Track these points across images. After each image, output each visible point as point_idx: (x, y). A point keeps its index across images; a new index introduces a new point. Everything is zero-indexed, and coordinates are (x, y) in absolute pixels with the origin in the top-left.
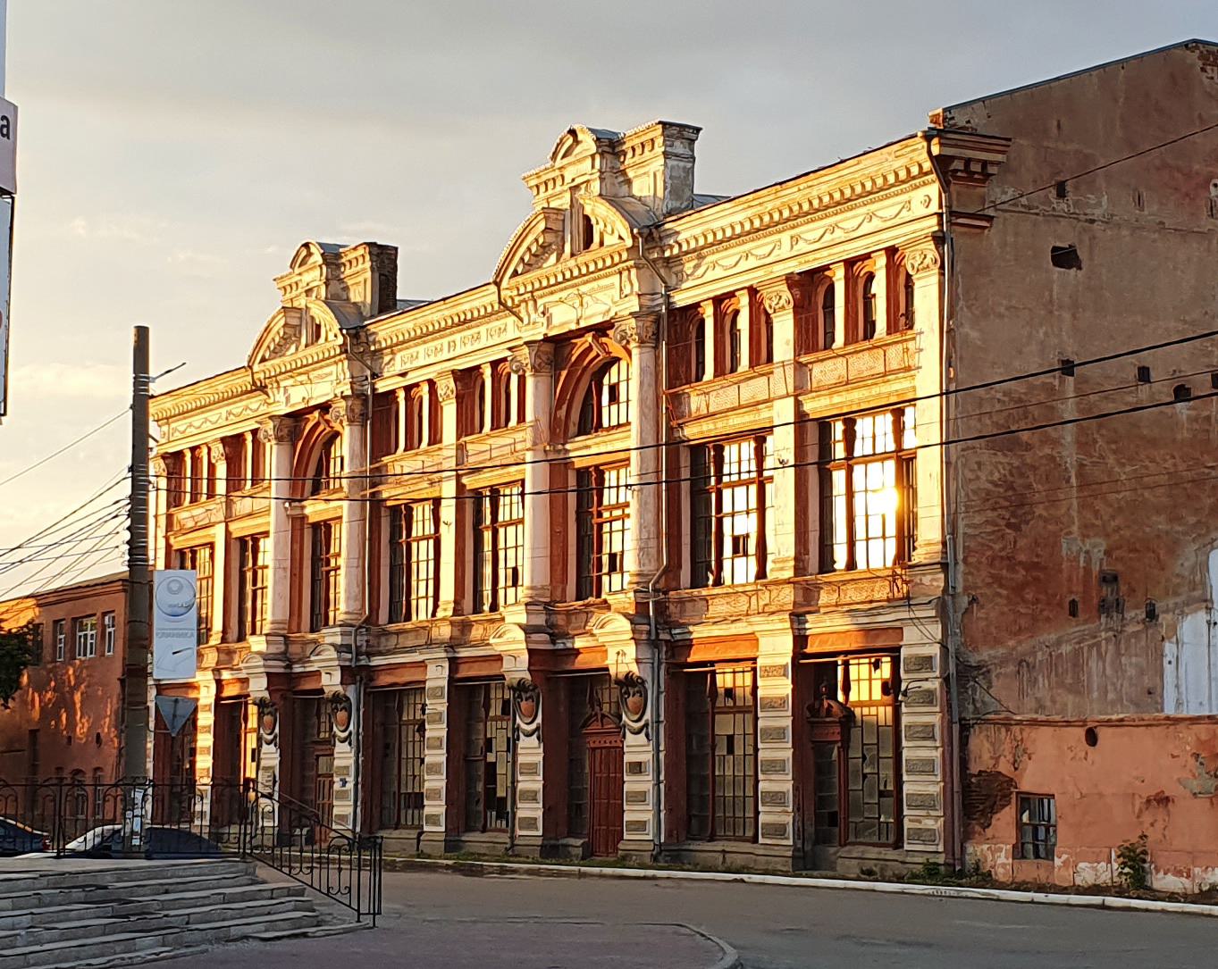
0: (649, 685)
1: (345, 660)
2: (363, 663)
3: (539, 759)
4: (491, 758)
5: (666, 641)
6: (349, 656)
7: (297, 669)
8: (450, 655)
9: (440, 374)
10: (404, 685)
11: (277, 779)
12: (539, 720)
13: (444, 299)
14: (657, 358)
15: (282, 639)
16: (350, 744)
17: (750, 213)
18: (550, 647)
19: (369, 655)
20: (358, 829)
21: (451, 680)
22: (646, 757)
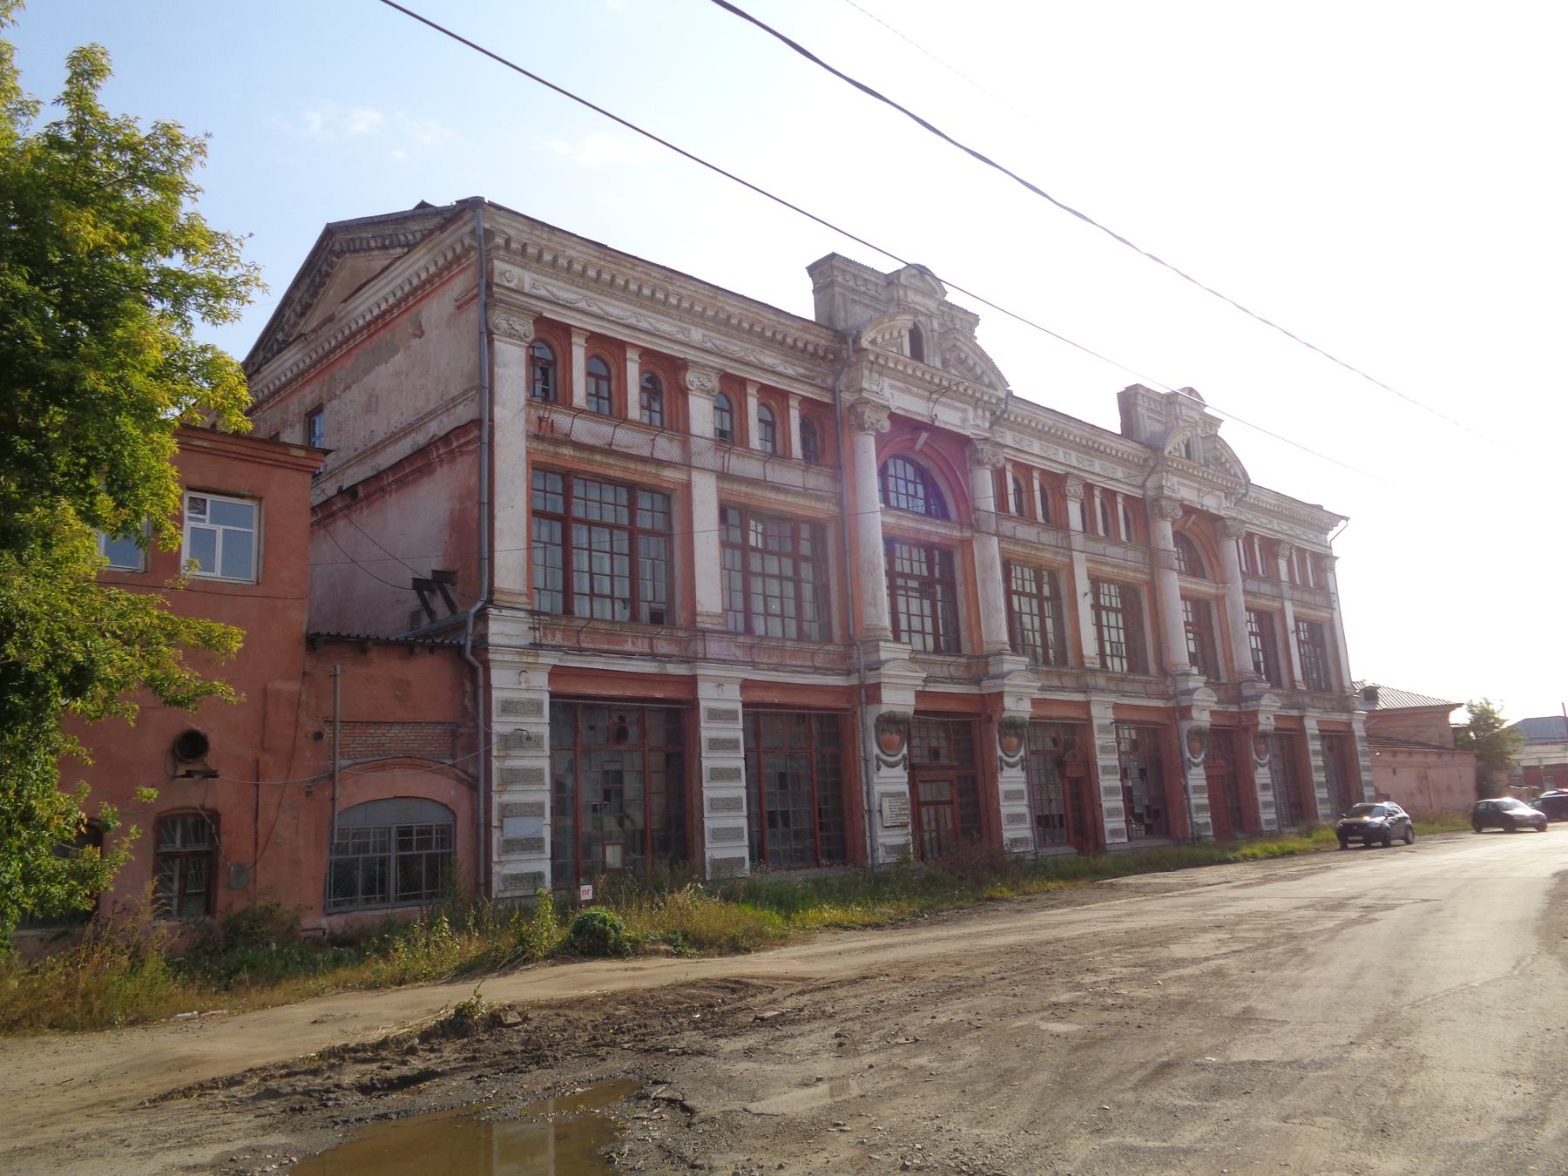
8: (1115, 700)
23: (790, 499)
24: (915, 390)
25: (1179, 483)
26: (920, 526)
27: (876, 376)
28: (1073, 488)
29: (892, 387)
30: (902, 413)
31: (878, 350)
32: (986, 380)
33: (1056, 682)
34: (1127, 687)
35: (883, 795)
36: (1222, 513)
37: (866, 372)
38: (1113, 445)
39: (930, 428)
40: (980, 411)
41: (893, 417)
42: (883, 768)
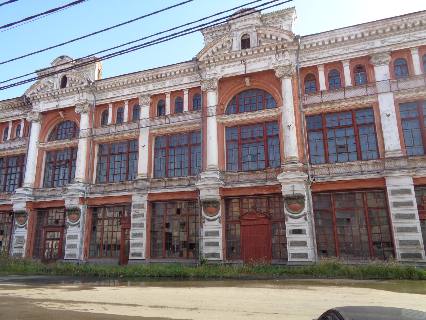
0: (306, 199)
1: (82, 195)
2: (89, 196)
3: (220, 231)
4: (170, 230)
5: (312, 183)
6: (83, 194)
7: (42, 200)
8: (149, 192)
9: (142, 96)
10: (111, 204)
11: (26, 241)
12: (220, 213)
13: (151, 70)
14: (293, 84)
15: (32, 189)
16: (79, 227)
17: (363, 31)
18: (223, 187)
19: (91, 194)
20: (82, 259)
21: (148, 202)
22: (307, 229)
23: (15, 150)
24: (52, 100)
25: (223, 68)
26: (60, 144)
27: (37, 103)
28: (141, 102)
29: (44, 103)
30: (46, 110)
31: (33, 96)
32: (80, 82)
33: (123, 188)
34: (174, 183)
35: (16, 237)
36: (271, 67)
37: (33, 104)
38: (171, 71)
39: (57, 110)
40: (81, 94)
41: (44, 114)
42: (17, 227)
